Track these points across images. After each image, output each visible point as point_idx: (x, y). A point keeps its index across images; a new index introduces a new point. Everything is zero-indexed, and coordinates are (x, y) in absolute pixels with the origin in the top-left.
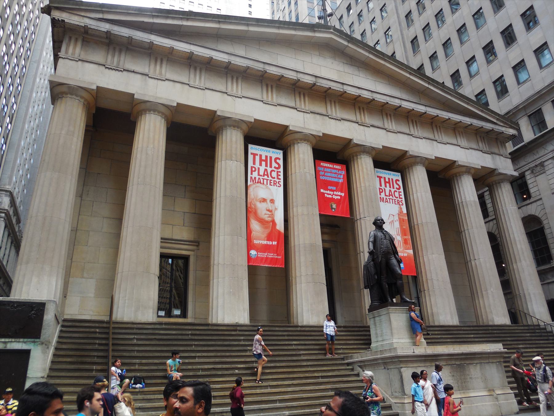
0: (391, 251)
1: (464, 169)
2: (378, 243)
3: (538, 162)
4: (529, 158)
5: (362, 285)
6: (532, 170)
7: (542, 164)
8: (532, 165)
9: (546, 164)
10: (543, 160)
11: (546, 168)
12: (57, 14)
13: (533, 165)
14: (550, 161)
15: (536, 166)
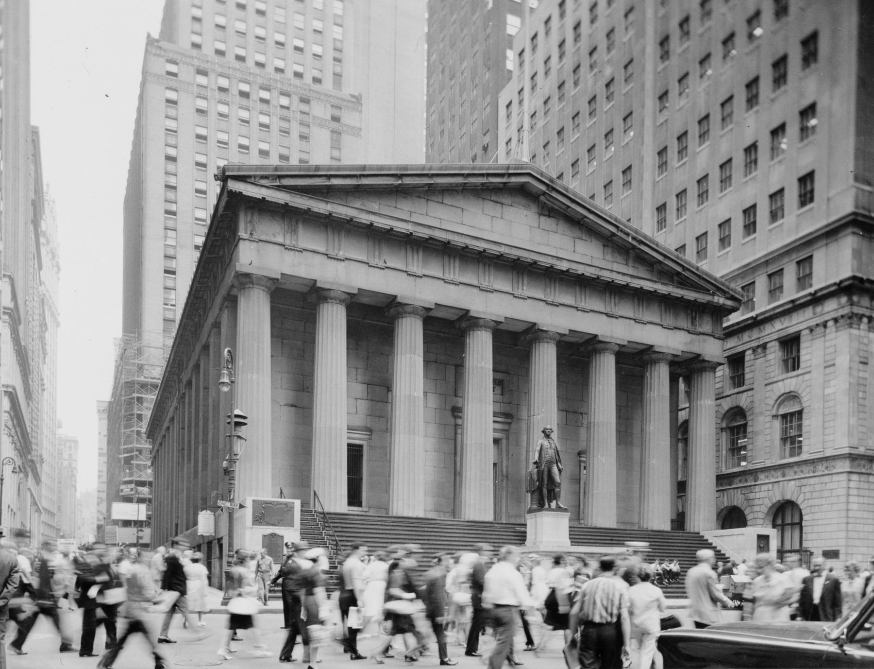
0: (554, 461)
1: (660, 356)
2: (543, 452)
3: (761, 342)
4: (755, 333)
5: (524, 490)
6: (754, 350)
7: (764, 346)
8: (754, 344)
9: (769, 345)
10: (766, 341)
11: (768, 351)
12: (235, 186)
13: (756, 344)
14: (774, 343)
15: (758, 346)
